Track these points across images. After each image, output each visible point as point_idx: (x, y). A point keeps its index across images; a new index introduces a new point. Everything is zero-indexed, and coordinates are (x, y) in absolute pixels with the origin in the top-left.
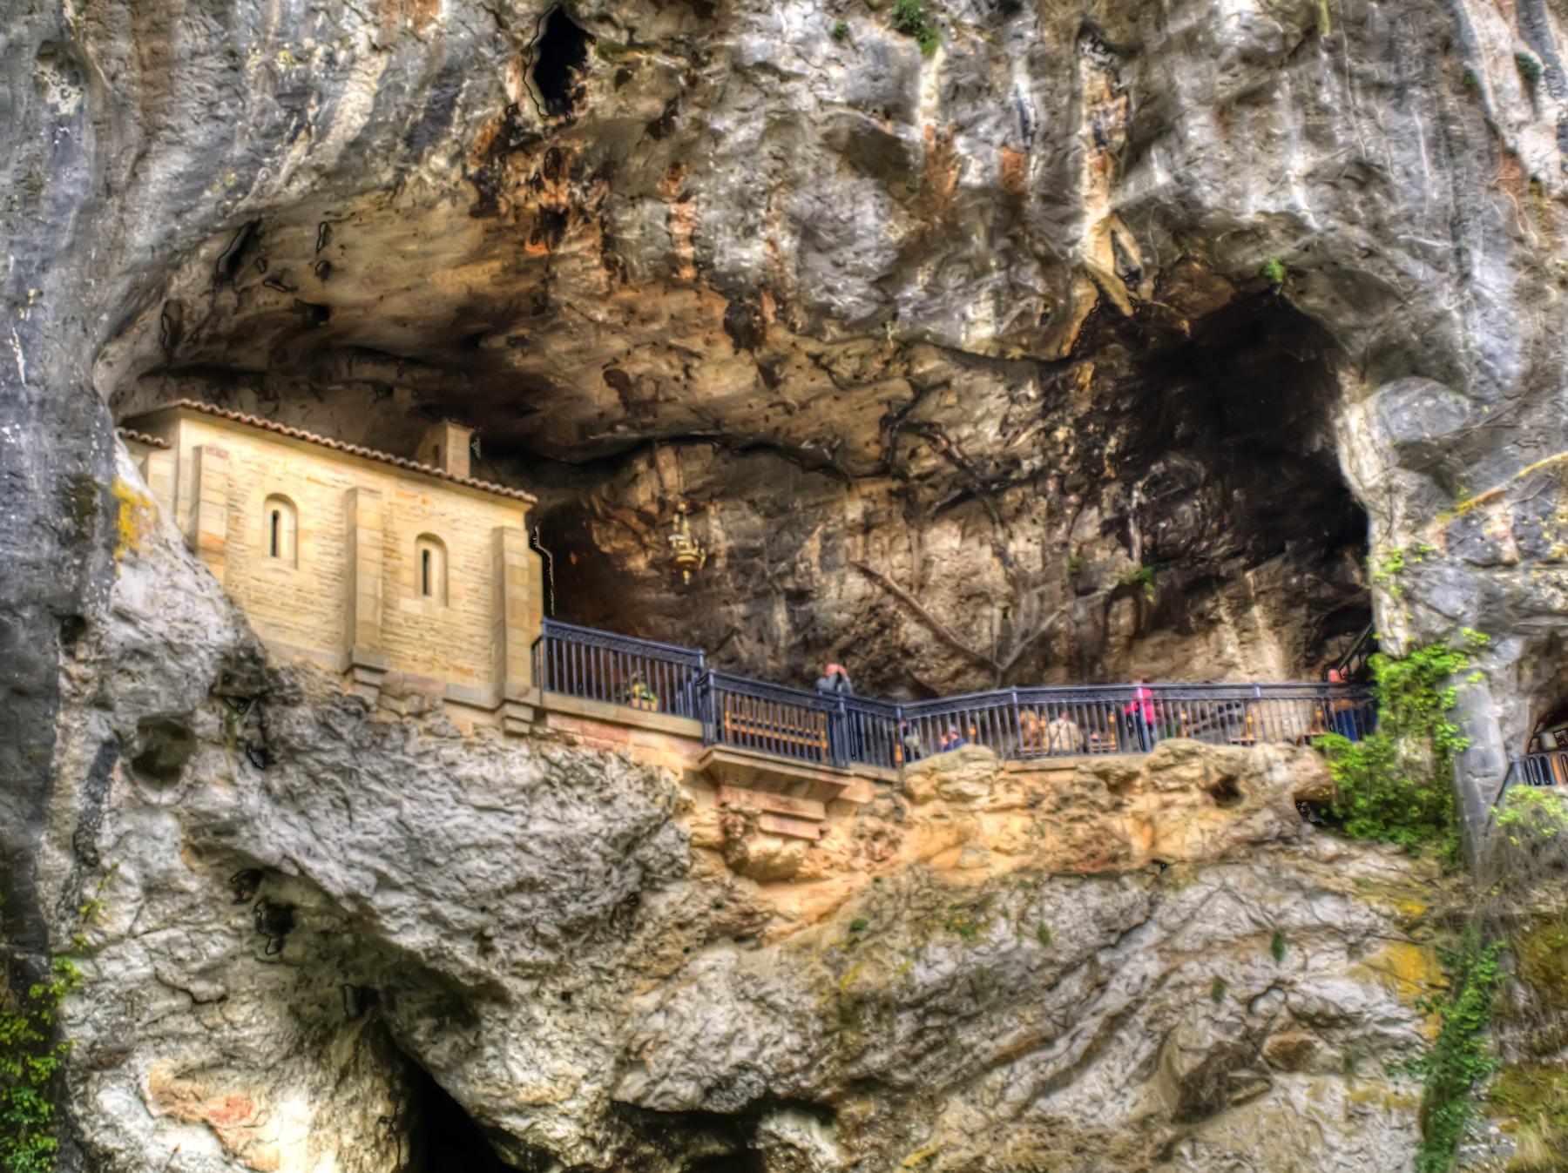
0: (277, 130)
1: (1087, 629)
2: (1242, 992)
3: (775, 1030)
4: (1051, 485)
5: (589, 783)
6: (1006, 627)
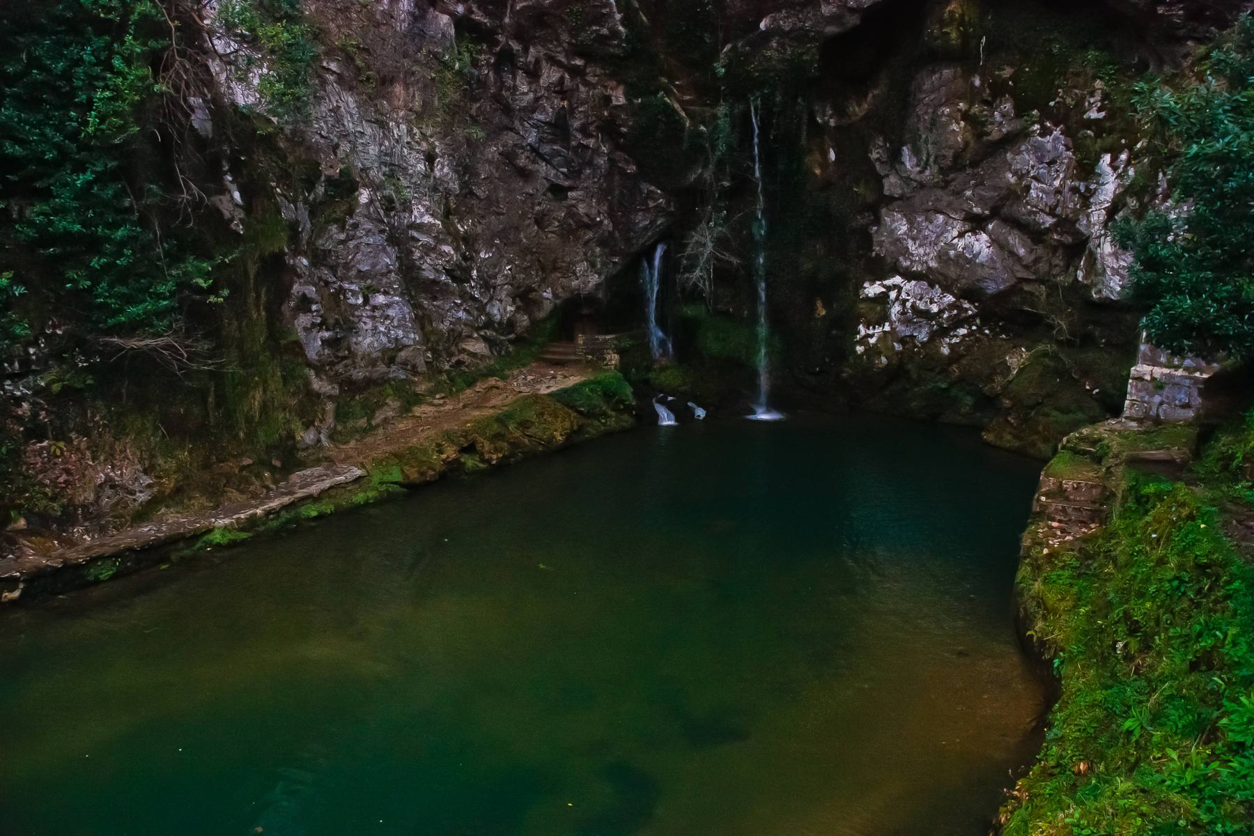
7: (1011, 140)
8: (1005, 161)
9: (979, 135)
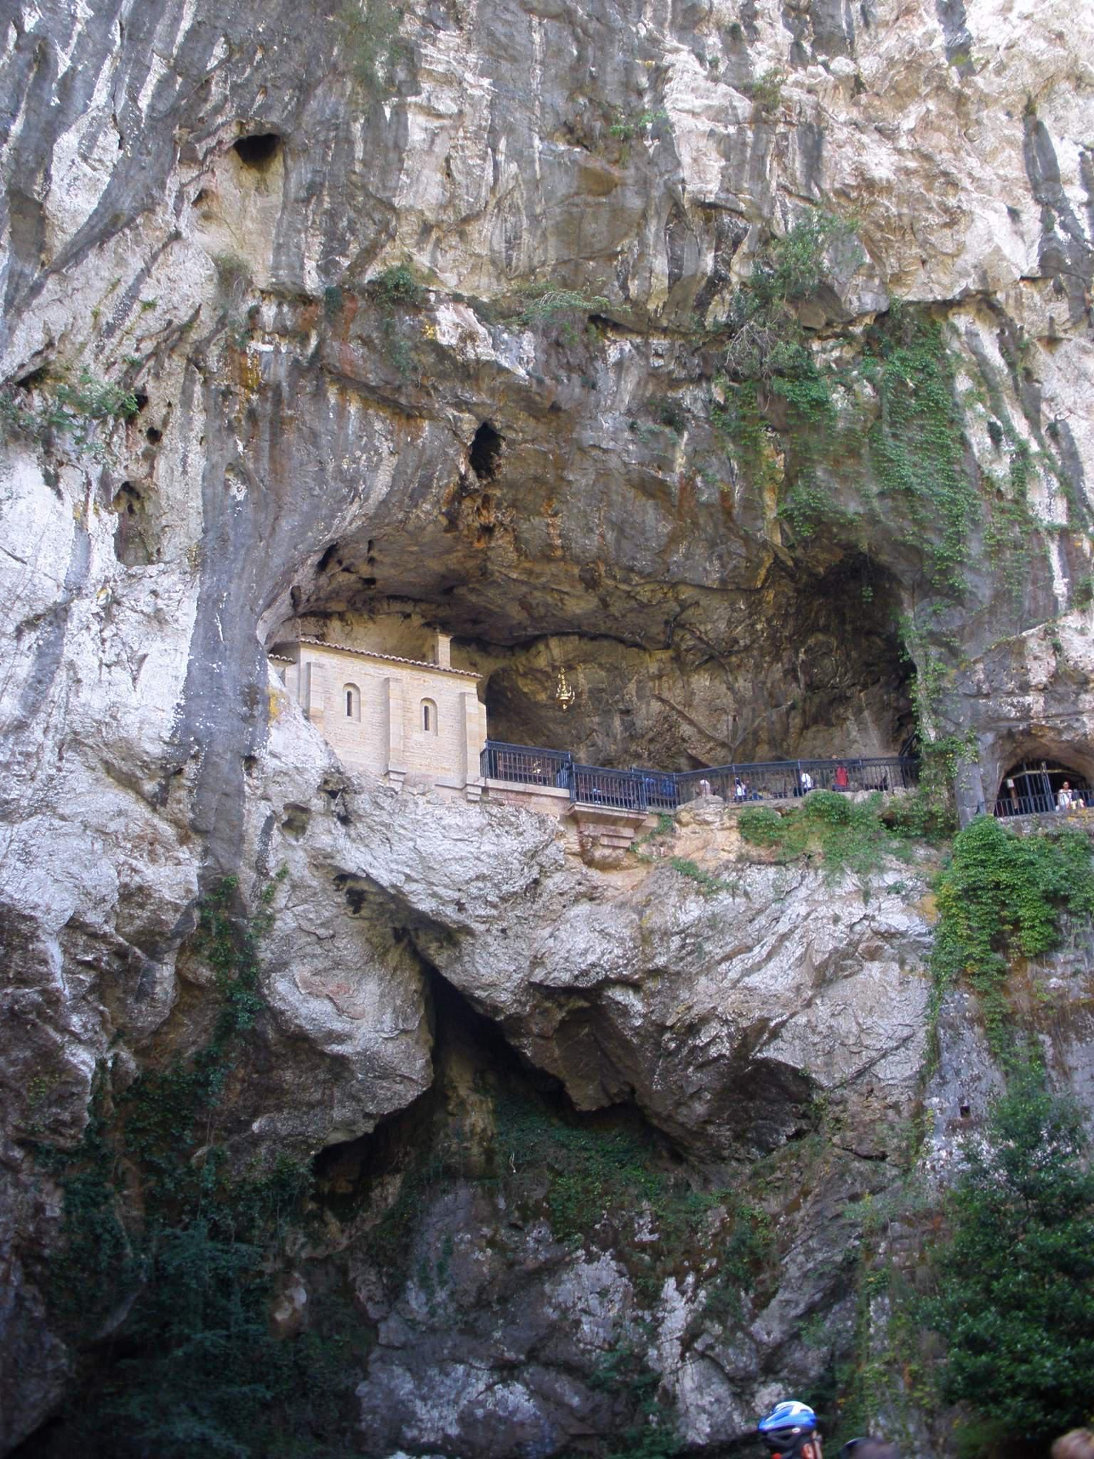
0: (344, 498)
1: (778, 726)
2: (846, 920)
3: (610, 947)
4: (755, 653)
5: (511, 824)
7: (552, 1269)
8: (543, 1294)
9: (511, 1265)
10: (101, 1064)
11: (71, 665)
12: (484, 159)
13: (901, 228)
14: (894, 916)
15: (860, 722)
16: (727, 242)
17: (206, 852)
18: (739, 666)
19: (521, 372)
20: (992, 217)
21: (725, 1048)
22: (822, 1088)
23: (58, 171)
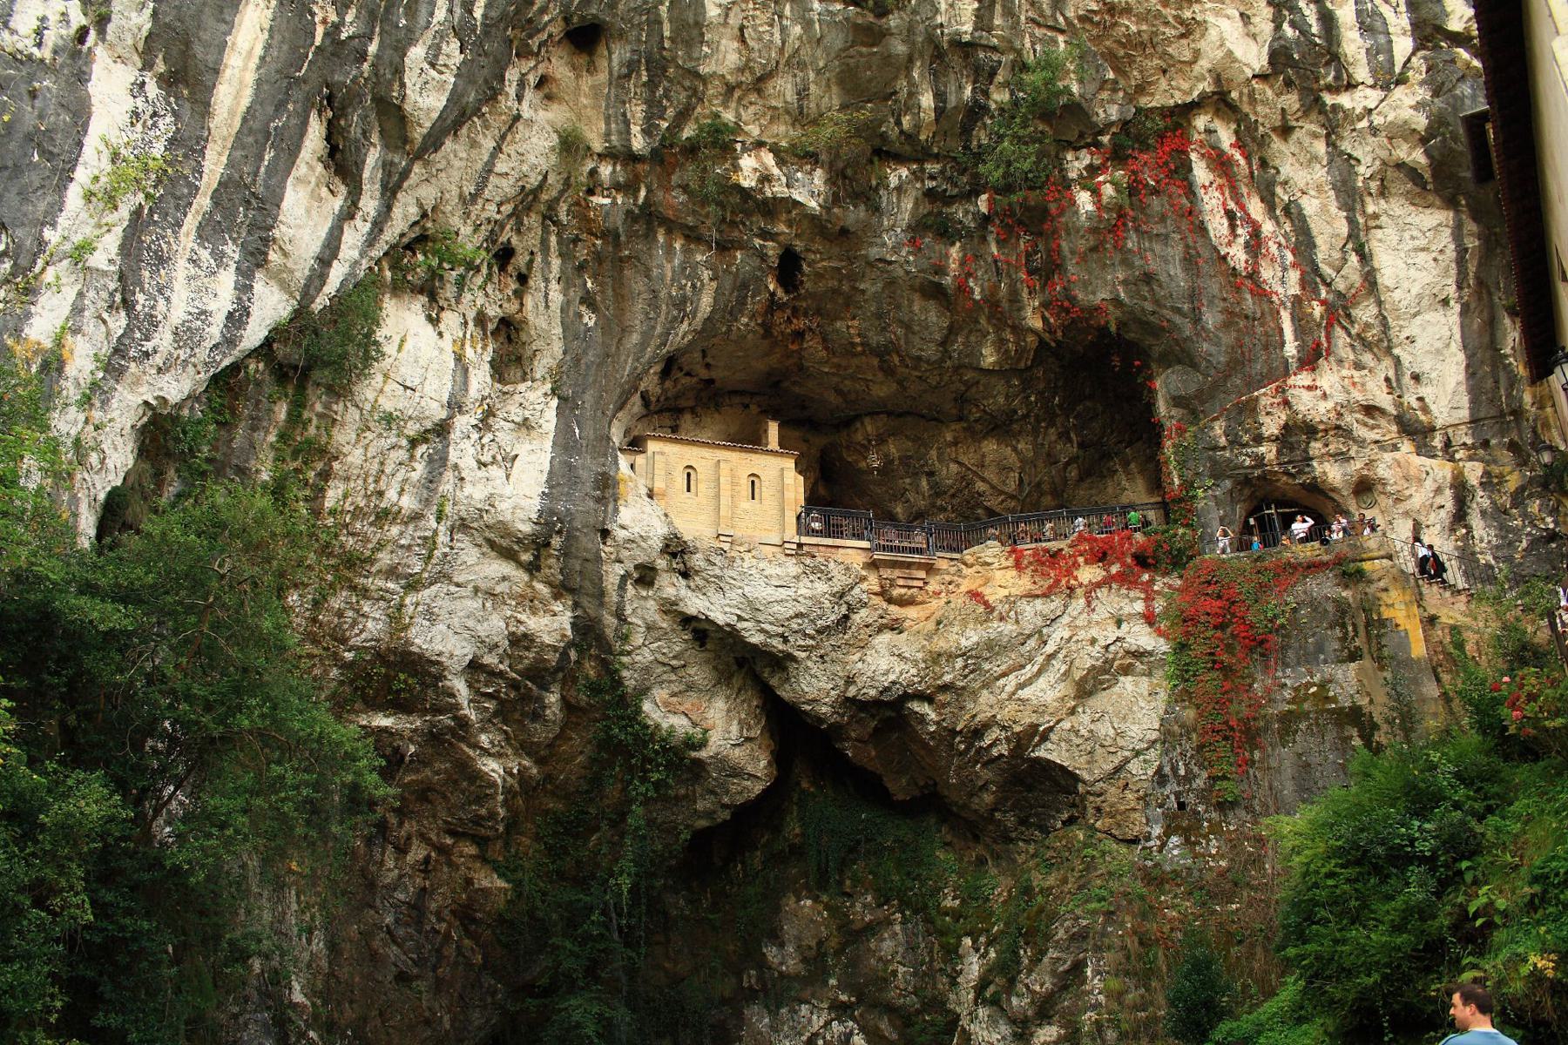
0: (675, 318)
6: (1021, 480)
8: (869, 949)
10: (509, 772)
11: (456, 467)
12: (771, 25)
13: (1142, 43)
14: (1143, 638)
15: (1128, 473)
16: (984, 76)
17: (576, 605)
18: (1020, 432)
19: (813, 204)
20: (1224, 24)
21: (1003, 749)
22: (1084, 782)
23: (411, 78)
